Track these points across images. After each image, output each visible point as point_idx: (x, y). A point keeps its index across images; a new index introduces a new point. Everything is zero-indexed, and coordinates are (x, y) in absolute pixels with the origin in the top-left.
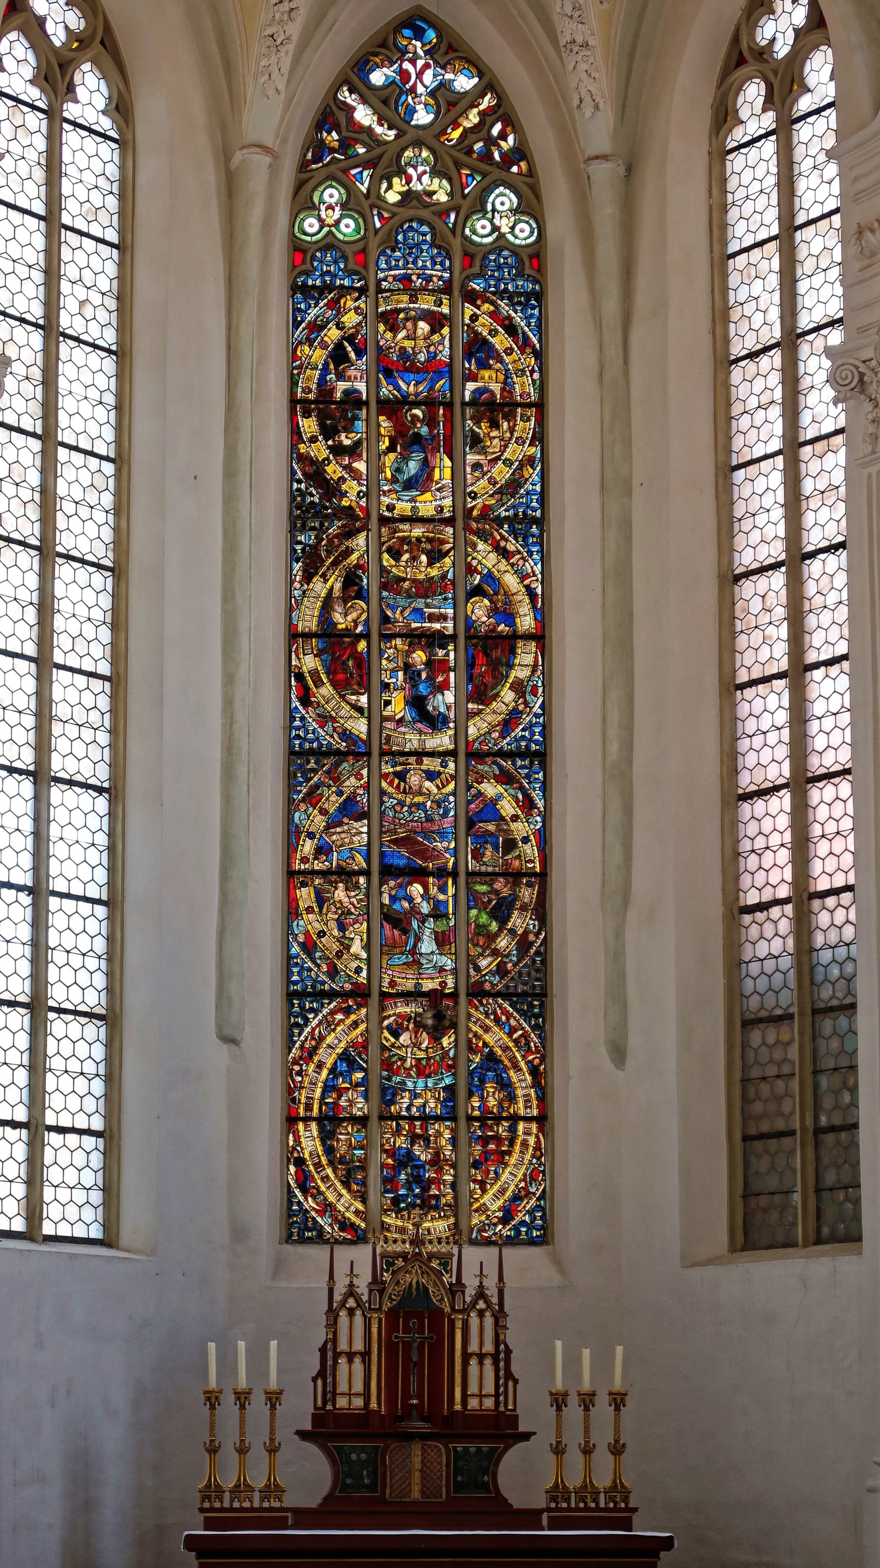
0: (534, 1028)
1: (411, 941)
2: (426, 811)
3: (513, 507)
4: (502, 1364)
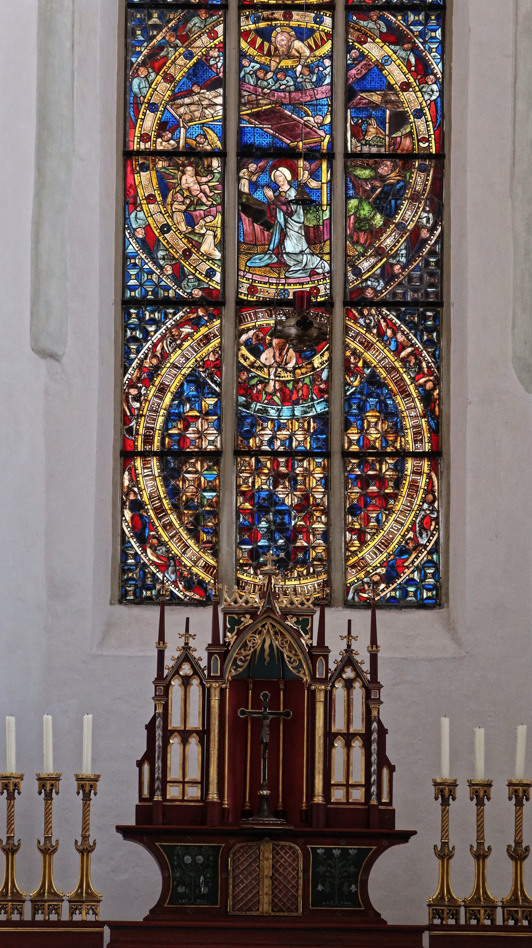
0: (427, 344)
1: (276, 238)
2: (295, 78)
4: (374, 747)
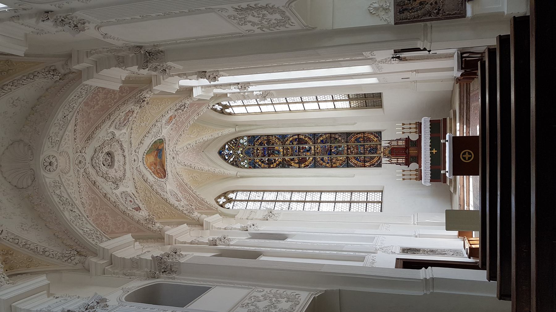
1: (340, 151)
3: (281, 139)
